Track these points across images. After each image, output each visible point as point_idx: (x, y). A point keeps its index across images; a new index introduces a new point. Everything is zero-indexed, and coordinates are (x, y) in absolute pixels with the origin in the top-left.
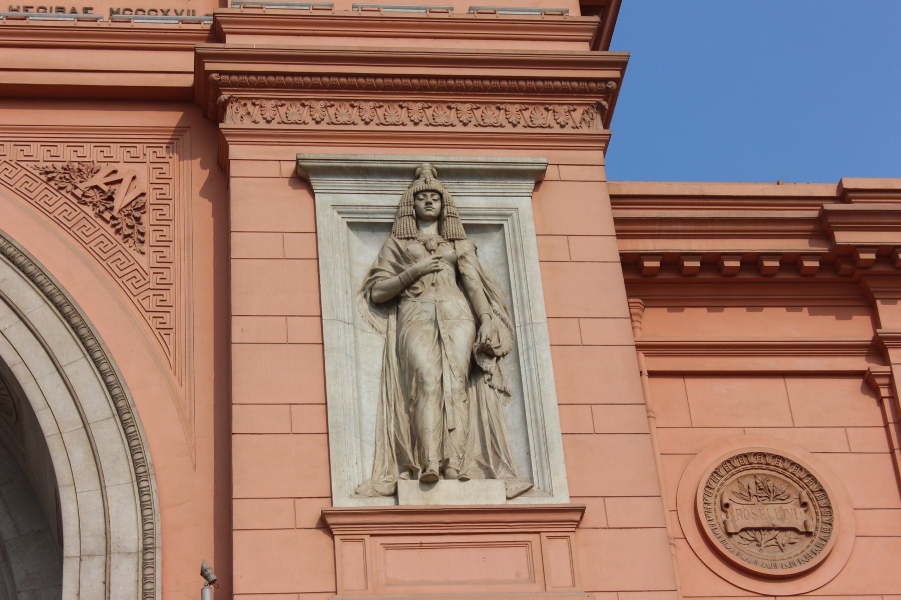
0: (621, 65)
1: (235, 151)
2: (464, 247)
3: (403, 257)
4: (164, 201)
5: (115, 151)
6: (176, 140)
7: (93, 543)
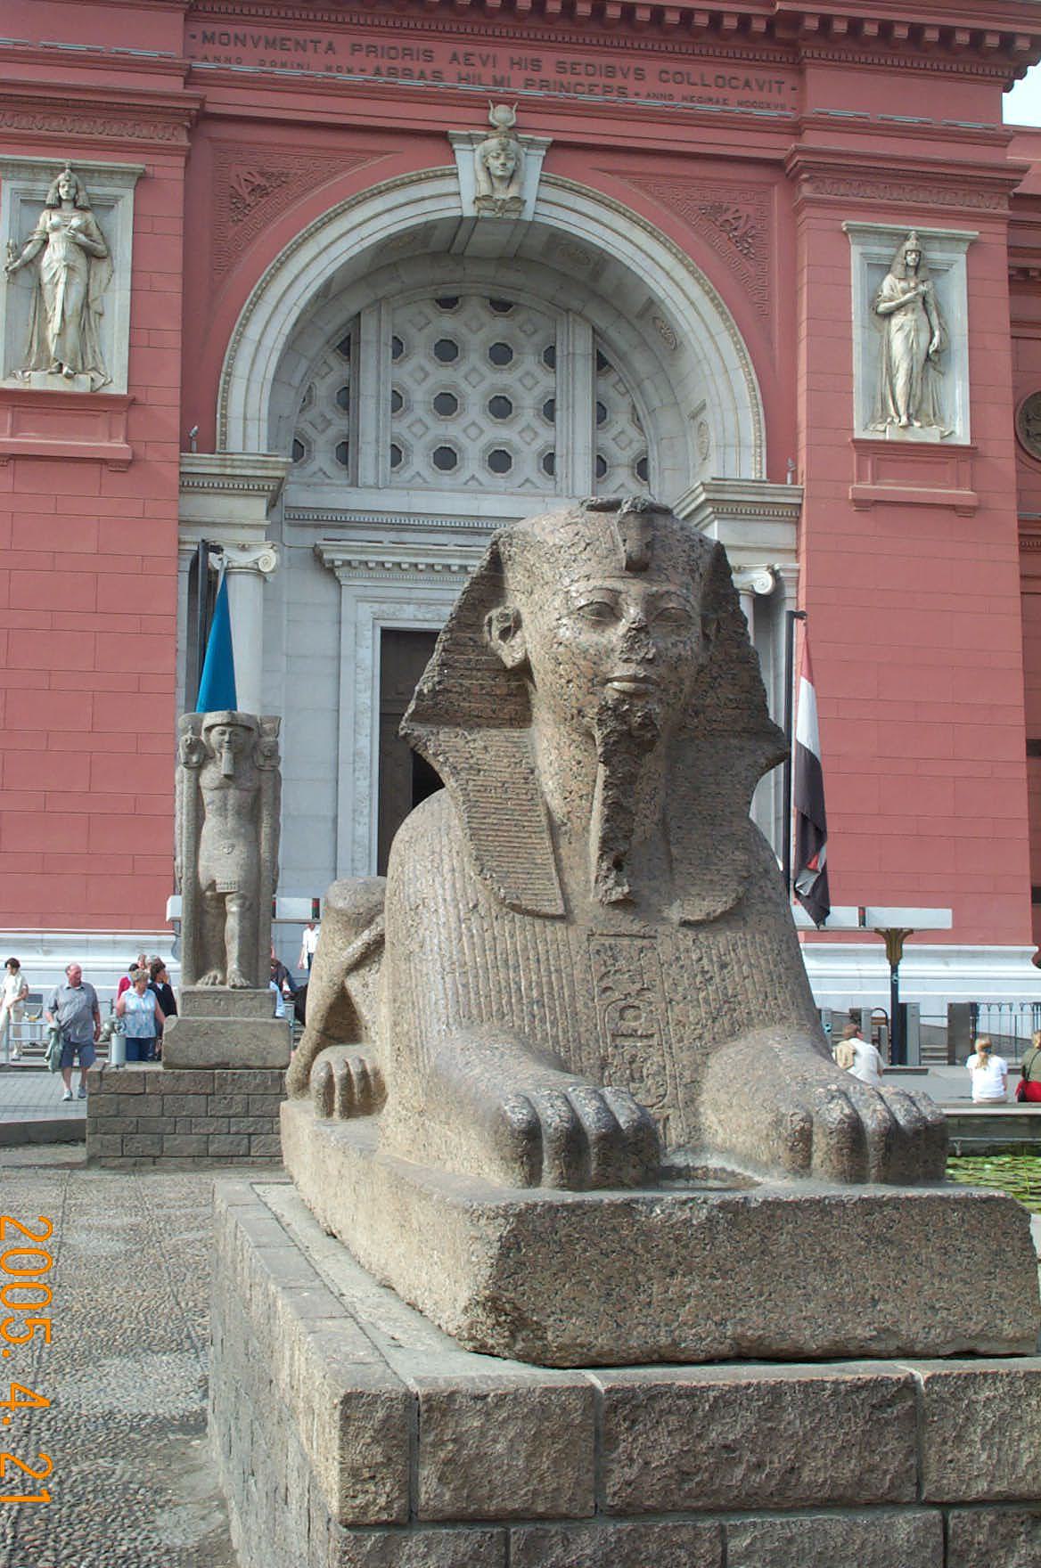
0: (1023, 170)
2: (930, 283)
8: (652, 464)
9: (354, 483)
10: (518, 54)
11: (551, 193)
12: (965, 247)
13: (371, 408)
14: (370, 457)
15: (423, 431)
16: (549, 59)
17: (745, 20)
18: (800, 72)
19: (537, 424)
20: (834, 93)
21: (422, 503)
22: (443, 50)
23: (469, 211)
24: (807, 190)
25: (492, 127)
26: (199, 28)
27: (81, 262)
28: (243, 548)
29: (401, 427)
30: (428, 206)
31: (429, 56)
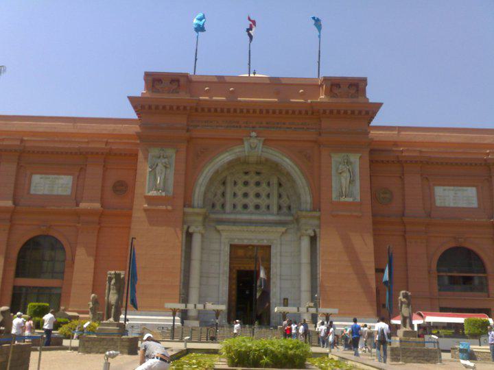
9: (225, 213)
11: (265, 150)
12: (358, 157)
13: (229, 196)
14: (228, 207)
15: (240, 200)
17: (307, 113)
18: (321, 121)
19: (265, 199)
21: (239, 217)
23: (247, 154)
25: (251, 137)
27: (164, 169)
28: (197, 227)
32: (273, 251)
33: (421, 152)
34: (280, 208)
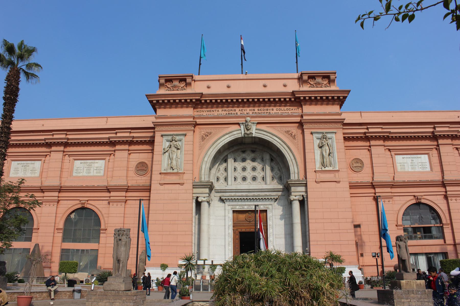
0: (344, 119)
1: (305, 130)
3: (322, 143)
4: (297, 134)
5: (292, 129)
6: (298, 127)
7: (293, 172)
8: (282, 178)
10: (250, 108)
11: (257, 131)
14: (230, 179)
15: (240, 174)
16: (256, 109)
17: (290, 99)
20: (308, 109)
21: (239, 187)
22: (237, 109)
24: (304, 127)
26: (196, 110)
27: (175, 150)
29: (236, 174)
30: (236, 135)
31: (235, 110)
32: (269, 214)
33: (382, 128)
34: (273, 178)
